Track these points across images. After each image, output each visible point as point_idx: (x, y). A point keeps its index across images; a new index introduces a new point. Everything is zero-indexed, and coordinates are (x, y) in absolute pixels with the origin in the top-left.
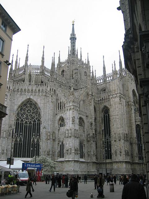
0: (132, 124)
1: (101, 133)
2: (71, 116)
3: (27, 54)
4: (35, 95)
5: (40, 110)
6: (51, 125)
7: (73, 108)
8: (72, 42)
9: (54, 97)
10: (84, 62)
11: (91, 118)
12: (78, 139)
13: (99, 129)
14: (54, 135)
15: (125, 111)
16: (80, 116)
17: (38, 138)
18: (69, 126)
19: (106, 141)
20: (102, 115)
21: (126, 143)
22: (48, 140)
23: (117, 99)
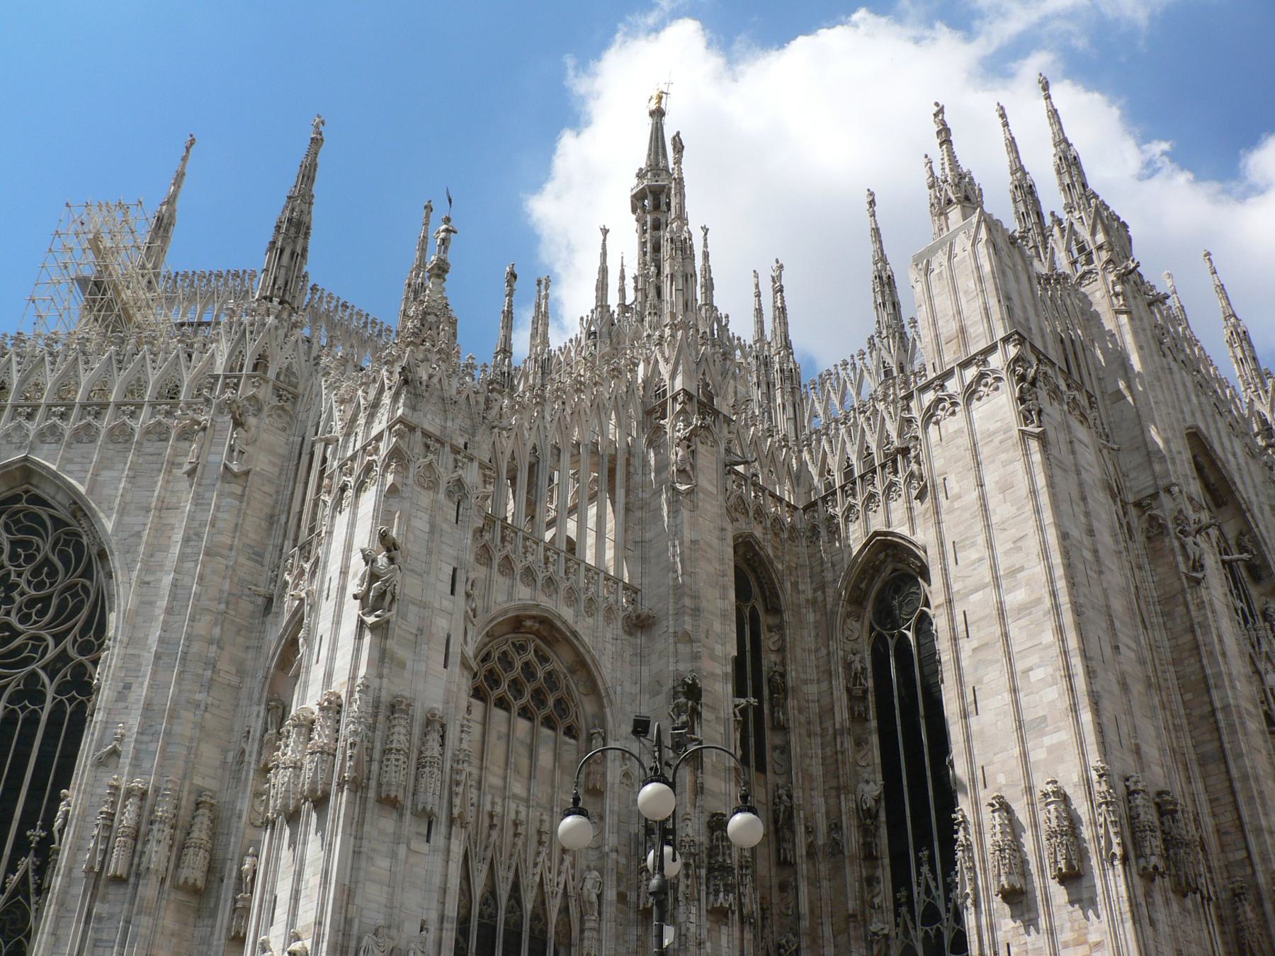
0: (1233, 730)
1: (852, 839)
2: (363, 537)
3: (171, 201)
4: (86, 434)
5: (109, 575)
6: (173, 715)
7: (395, 453)
8: (649, 218)
9: (267, 433)
10: (733, 329)
11: (689, 639)
12: (438, 838)
13: (819, 801)
14: (200, 833)
15: (1106, 539)
16: (524, 593)
17: (25, 877)
18: (329, 676)
19: (918, 934)
20: (856, 638)
21: (1161, 915)
22: (114, 893)
23: (998, 409)
